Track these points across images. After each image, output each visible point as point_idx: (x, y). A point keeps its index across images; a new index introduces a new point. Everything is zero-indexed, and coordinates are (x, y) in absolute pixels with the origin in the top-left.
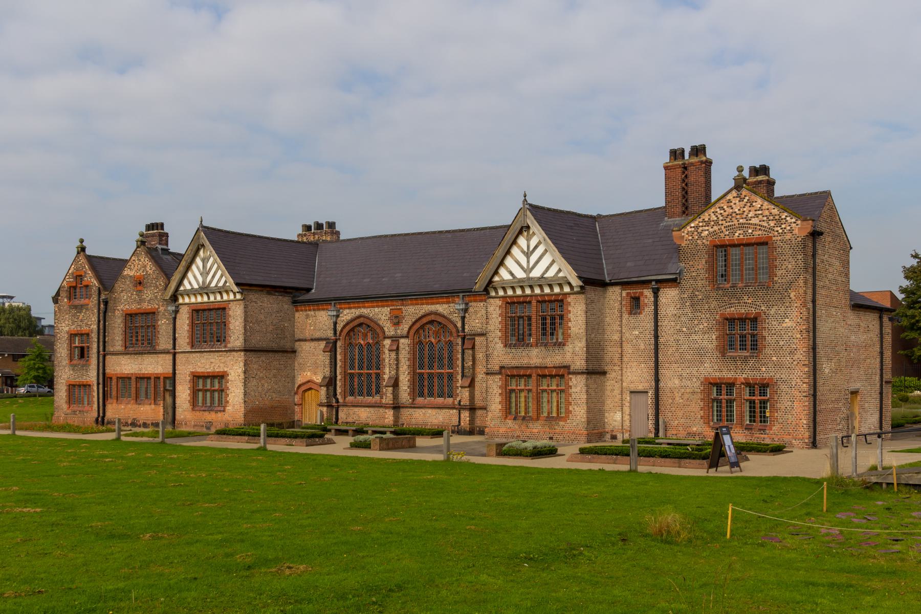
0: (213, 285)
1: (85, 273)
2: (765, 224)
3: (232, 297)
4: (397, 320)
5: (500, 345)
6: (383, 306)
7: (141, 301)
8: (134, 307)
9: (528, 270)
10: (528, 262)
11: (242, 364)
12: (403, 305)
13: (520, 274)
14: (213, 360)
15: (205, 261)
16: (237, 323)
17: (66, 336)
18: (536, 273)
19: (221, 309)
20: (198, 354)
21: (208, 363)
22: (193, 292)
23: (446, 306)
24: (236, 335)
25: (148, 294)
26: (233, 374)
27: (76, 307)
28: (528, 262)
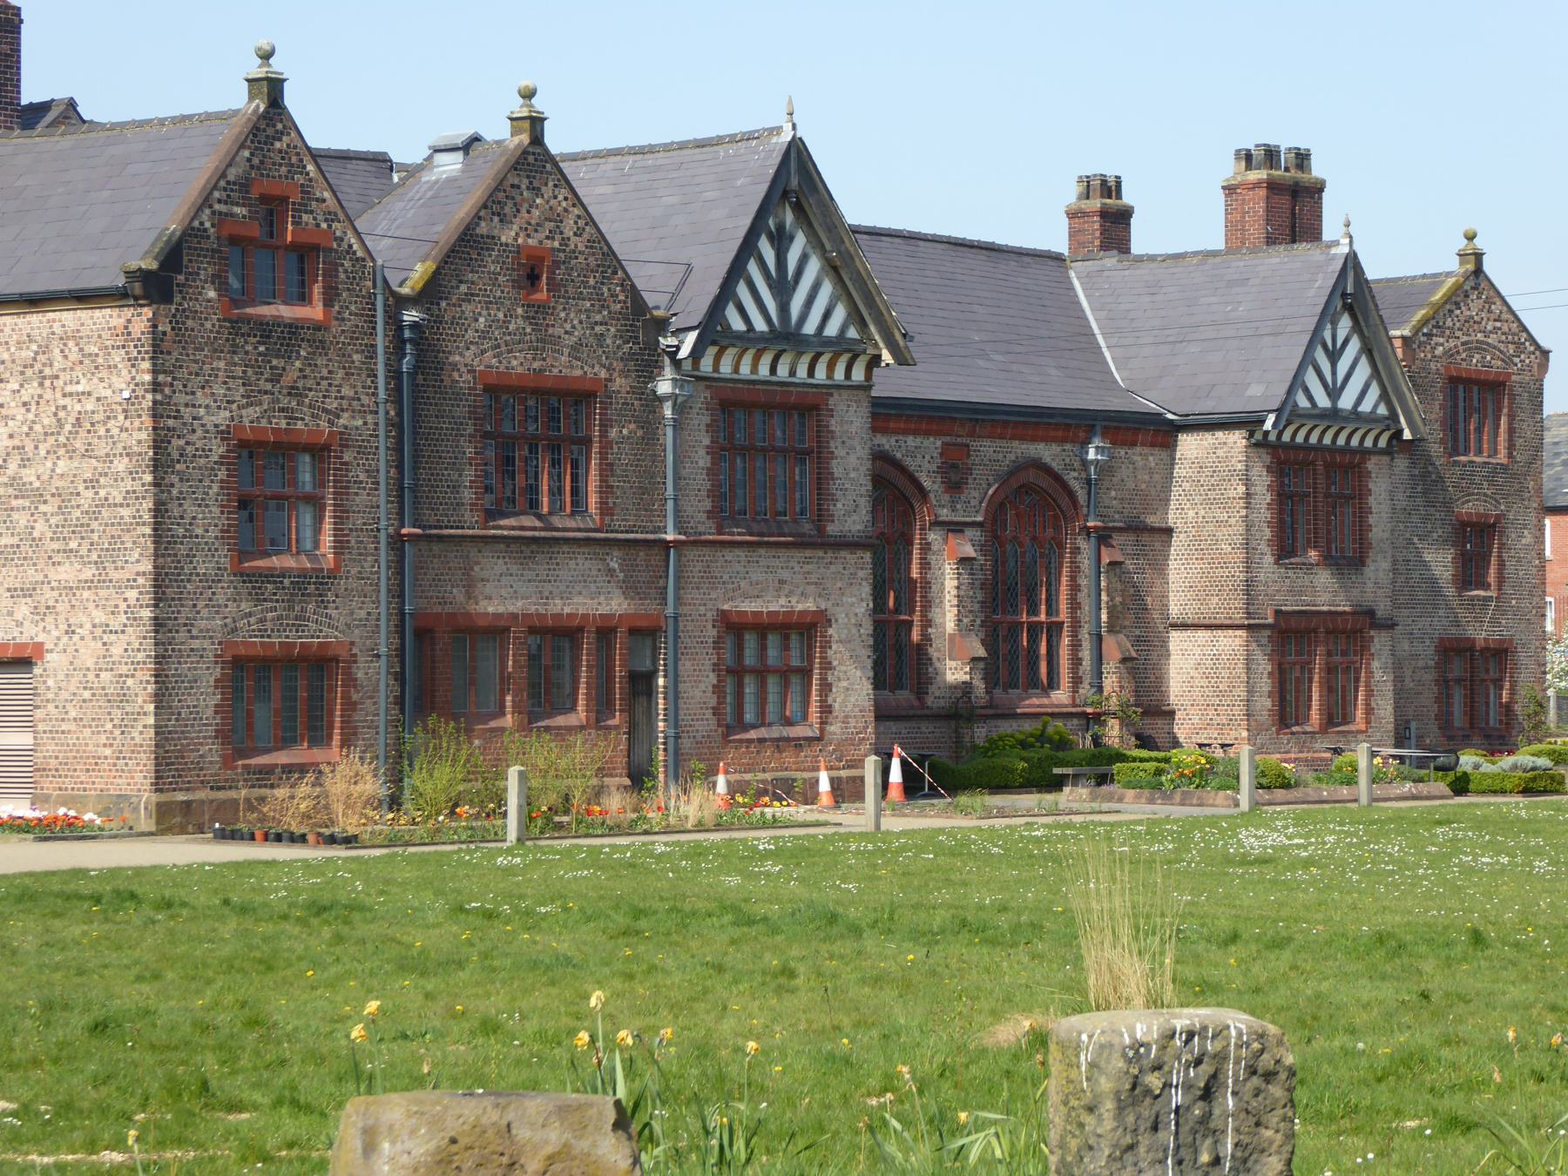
0: (810, 328)
1: (306, 192)
2: (1502, 347)
3: (839, 374)
4: (955, 476)
5: (1269, 559)
6: (928, 433)
7: (545, 343)
8: (518, 364)
9: (1334, 393)
10: (1334, 373)
11: (866, 589)
12: (972, 434)
13: (1323, 401)
14: (785, 574)
15: (781, 241)
16: (852, 459)
17: (218, 449)
18: (1346, 402)
19: (807, 407)
20: (741, 553)
21: (771, 588)
22: (748, 339)
23: (1055, 448)
24: (851, 496)
25: (570, 324)
26: (842, 618)
27: (265, 329)
28: (1334, 373)
